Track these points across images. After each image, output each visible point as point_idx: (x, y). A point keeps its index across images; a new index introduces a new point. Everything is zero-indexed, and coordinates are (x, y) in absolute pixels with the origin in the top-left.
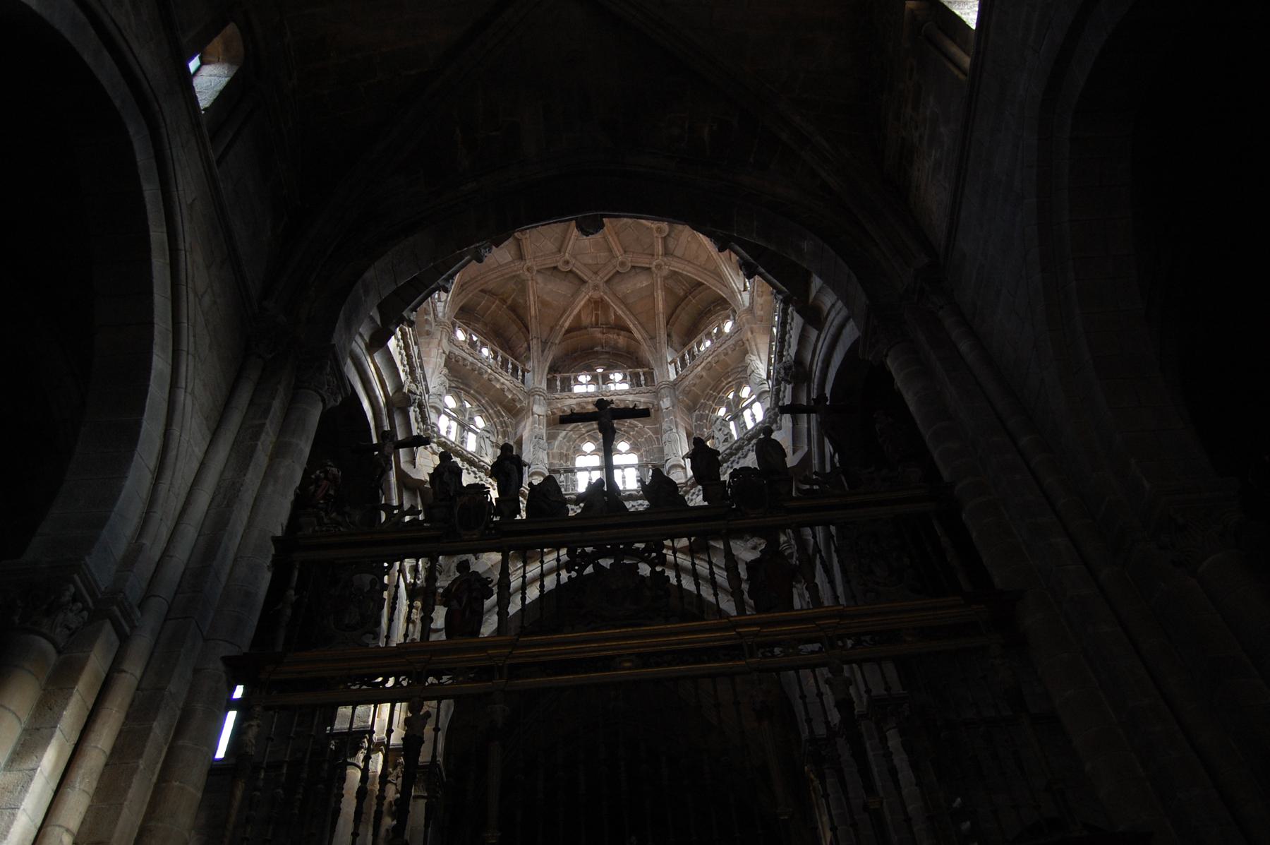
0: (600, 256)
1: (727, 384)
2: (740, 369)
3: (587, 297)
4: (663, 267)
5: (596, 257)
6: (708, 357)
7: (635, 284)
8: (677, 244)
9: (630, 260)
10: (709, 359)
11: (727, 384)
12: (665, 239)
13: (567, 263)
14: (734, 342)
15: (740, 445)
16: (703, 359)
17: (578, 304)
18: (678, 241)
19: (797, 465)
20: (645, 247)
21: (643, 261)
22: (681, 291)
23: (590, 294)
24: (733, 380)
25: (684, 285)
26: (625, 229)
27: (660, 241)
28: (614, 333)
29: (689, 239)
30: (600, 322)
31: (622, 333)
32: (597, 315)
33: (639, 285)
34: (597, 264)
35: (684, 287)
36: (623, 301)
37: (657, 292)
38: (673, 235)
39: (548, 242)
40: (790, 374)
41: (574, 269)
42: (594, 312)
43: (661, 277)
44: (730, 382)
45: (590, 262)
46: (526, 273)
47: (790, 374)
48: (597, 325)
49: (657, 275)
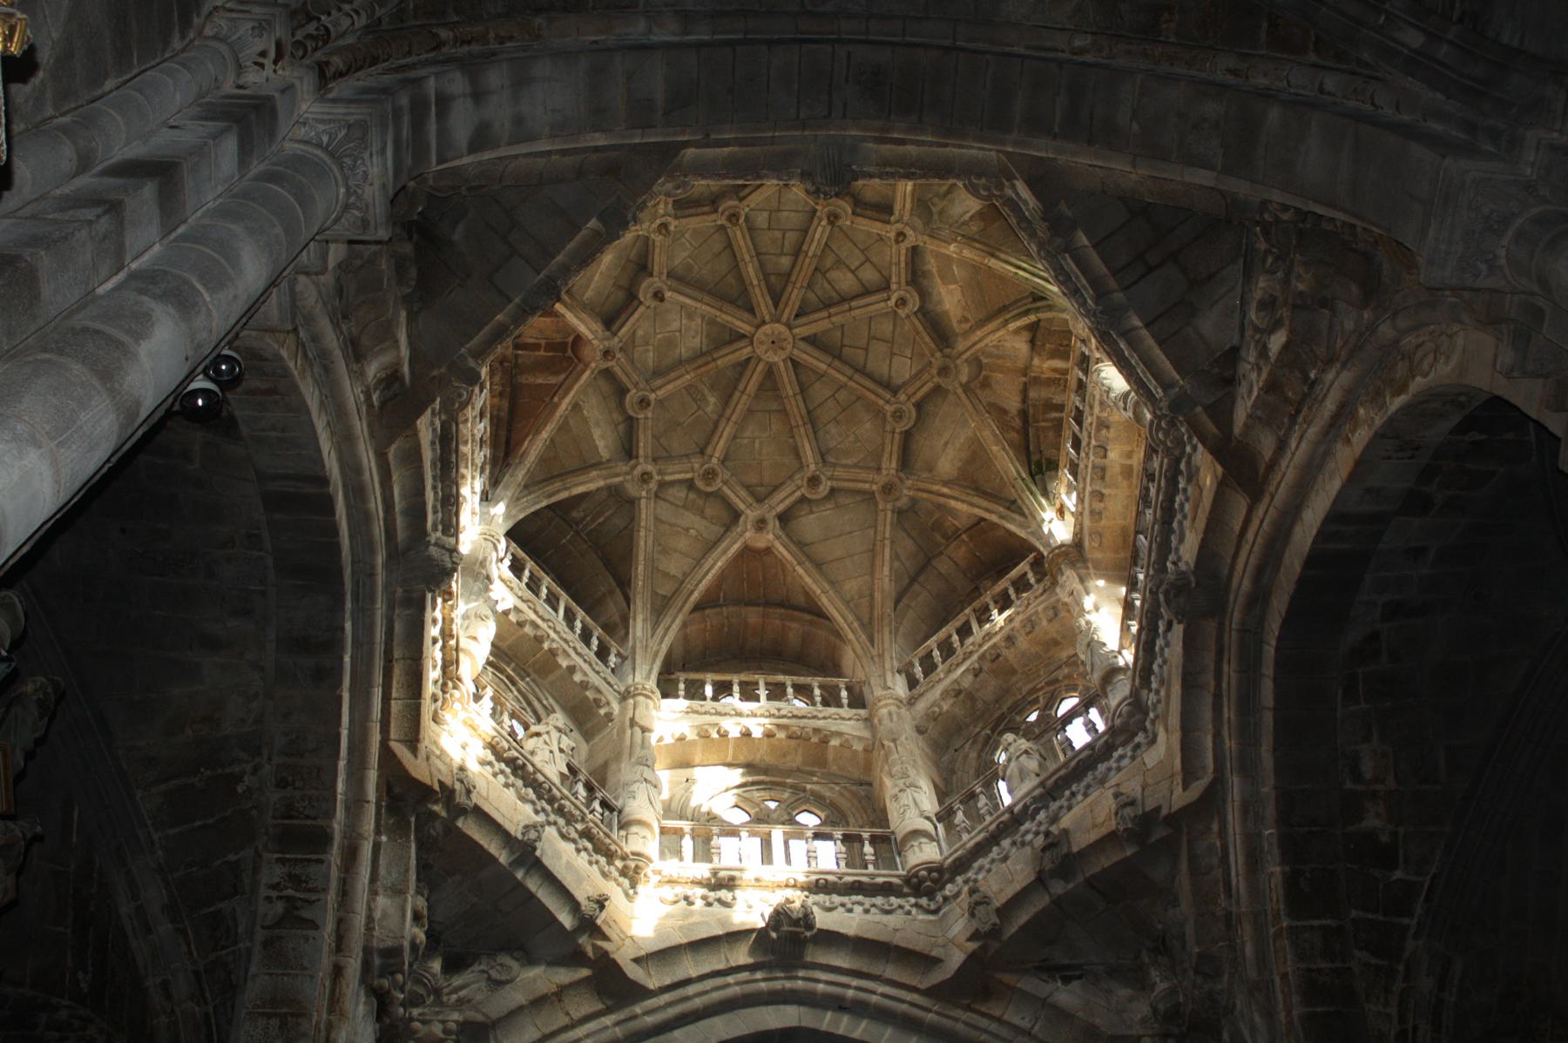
0: (648, 350)
1: (509, 677)
2: (545, 702)
3: (591, 336)
4: (645, 486)
5: (647, 344)
6: (555, 631)
7: (597, 424)
8: (677, 506)
9: (645, 417)
10: (553, 635)
11: (509, 677)
12: (690, 485)
13: (659, 296)
14: (596, 684)
15: (573, 816)
16: (549, 620)
17: (580, 320)
18: (684, 507)
19: (629, 979)
20: (662, 440)
21: (644, 444)
22: (582, 514)
23: (595, 342)
24: (519, 691)
25: (593, 520)
26: (694, 399)
27: (689, 476)
28: (503, 385)
29: (692, 531)
30: (520, 352)
31: (505, 404)
32: (536, 347)
33: (597, 433)
34: (634, 347)
35: (588, 518)
36: (576, 407)
37: (599, 476)
38: (692, 496)
39: (686, 254)
40: (798, 929)
41: (642, 309)
42: (543, 342)
43: (621, 482)
44: (514, 683)
45: (640, 333)
46: (658, 222)
47: (798, 929)
48: (517, 347)
49: (627, 473)
